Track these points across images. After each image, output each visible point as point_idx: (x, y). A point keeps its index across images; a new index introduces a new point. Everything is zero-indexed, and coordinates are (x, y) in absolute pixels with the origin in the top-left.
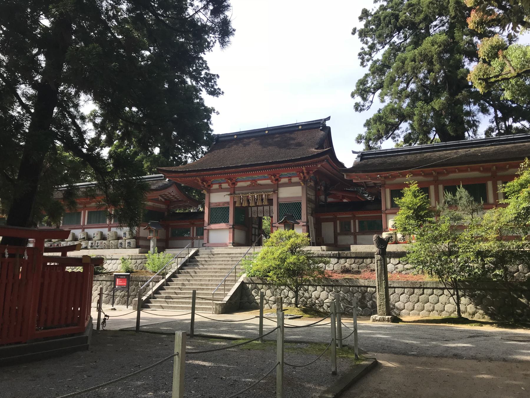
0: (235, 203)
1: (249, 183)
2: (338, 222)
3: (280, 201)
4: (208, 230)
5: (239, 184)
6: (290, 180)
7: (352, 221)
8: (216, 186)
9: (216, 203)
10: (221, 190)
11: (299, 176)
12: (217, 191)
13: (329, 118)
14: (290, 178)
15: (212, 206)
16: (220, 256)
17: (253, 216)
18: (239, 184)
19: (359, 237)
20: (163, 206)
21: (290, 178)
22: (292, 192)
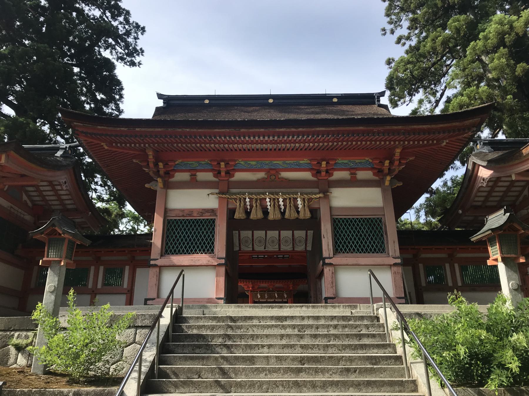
0: (231, 212)
1: (261, 175)
2: (421, 266)
4: (161, 267)
5: (239, 176)
7: (447, 266)
9: (183, 210)
15: (172, 217)
16: (255, 322)
17: (244, 248)
18: (239, 176)
21: (353, 170)
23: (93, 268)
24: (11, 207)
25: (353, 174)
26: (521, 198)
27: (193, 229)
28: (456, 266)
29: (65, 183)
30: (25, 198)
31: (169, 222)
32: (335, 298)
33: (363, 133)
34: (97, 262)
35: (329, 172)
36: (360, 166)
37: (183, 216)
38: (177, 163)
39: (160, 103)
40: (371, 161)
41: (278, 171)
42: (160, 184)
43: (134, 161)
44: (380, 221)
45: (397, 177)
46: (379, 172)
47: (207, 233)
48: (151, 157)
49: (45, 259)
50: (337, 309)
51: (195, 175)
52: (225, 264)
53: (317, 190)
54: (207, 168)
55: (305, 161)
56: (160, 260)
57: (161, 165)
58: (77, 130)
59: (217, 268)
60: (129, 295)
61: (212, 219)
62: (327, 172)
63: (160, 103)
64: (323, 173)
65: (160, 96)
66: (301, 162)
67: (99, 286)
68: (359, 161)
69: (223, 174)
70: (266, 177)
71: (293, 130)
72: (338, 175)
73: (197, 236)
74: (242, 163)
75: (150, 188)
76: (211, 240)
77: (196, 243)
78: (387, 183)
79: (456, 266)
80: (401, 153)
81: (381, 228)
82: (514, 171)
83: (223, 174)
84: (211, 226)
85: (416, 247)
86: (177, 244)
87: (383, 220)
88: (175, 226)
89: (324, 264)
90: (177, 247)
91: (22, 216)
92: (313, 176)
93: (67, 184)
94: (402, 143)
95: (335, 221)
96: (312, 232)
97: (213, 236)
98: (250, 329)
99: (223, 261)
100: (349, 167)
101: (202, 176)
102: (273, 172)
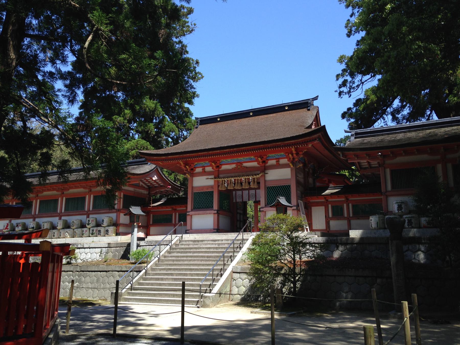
1: (234, 166)
2: (330, 206)
3: (267, 184)
5: (224, 167)
6: (278, 162)
7: (345, 205)
8: (199, 170)
10: (204, 173)
11: (287, 157)
12: (199, 174)
13: (316, 98)
14: (278, 160)
16: (206, 242)
17: (238, 200)
18: (224, 167)
19: (353, 222)
20: (146, 192)
22: (281, 174)
30: (141, 183)
41: (241, 163)
53: (259, 172)
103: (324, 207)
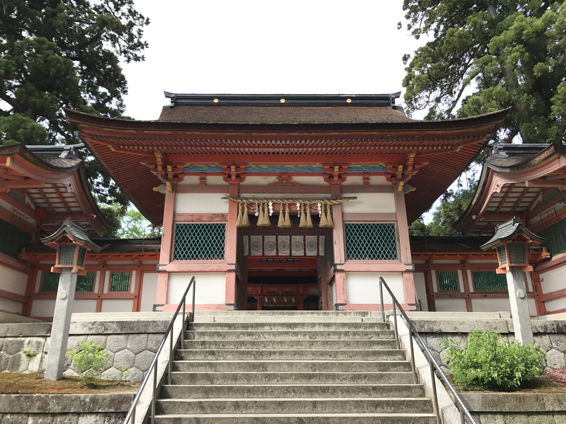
1: (273, 179)
2: (433, 272)
5: (250, 180)
9: (192, 215)
15: (181, 221)
16: (267, 329)
18: (250, 180)
19: (474, 302)
21: (366, 175)
23: (98, 273)
24: (14, 210)
25: (366, 179)
26: (534, 205)
27: (202, 234)
28: (469, 272)
29: (70, 185)
30: (28, 200)
31: (178, 227)
32: (346, 304)
33: (377, 137)
34: (103, 267)
35: (341, 177)
36: (373, 171)
37: (193, 221)
38: (185, 166)
39: (168, 102)
40: (384, 166)
41: (290, 175)
42: (168, 188)
43: (142, 163)
44: (393, 227)
45: (410, 183)
46: (392, 177)
47: (217, 238)
48: (159, 160)
49: (56, 266)
50: (348, 316)
51: (205, 179)
52: (236, 271)
54: (217, 171)
55: (317, 165)
56: (169, 265)
57: (169, 168)
58: (84, 132)
59: (227, 274)
60: (136, 300)
61: (221, 224)
62: (340, 176)
63: (168, 102)
64: (336, 178)
65: (167, 95)
66: (314, 166)
67: (106, 291)
68: (372, 166)
69: (233, 177)
70: (277, 181)
71: (306, 134)
72: (351, 180)
73: (206, 242)
74: (253, 166)
75: (158, 192)
76: (221, 245)
77: (206, 249)
78: (400, 189)
79: (469, 272)
80: (415, 158)
81: (393, 234)
82: (526, 178)
83: (233, 177)
84: (221, 231)
85: (429, 253)
86: (187, 249)
87: (395, 227)
88: (184, 231)
89: (336, 270)
90: (187, 253)
91: (25, 219)
92: (325, 180)
93: (71, 187)
94: (416, 148)
95: (347, 227)
96: (324, 237)
97: (223, 241)
98: (261, 336)
99: (233, 267)
100: (362, 172)
101: (212, 180)
102: (285, 177)
103: (423, 274)
